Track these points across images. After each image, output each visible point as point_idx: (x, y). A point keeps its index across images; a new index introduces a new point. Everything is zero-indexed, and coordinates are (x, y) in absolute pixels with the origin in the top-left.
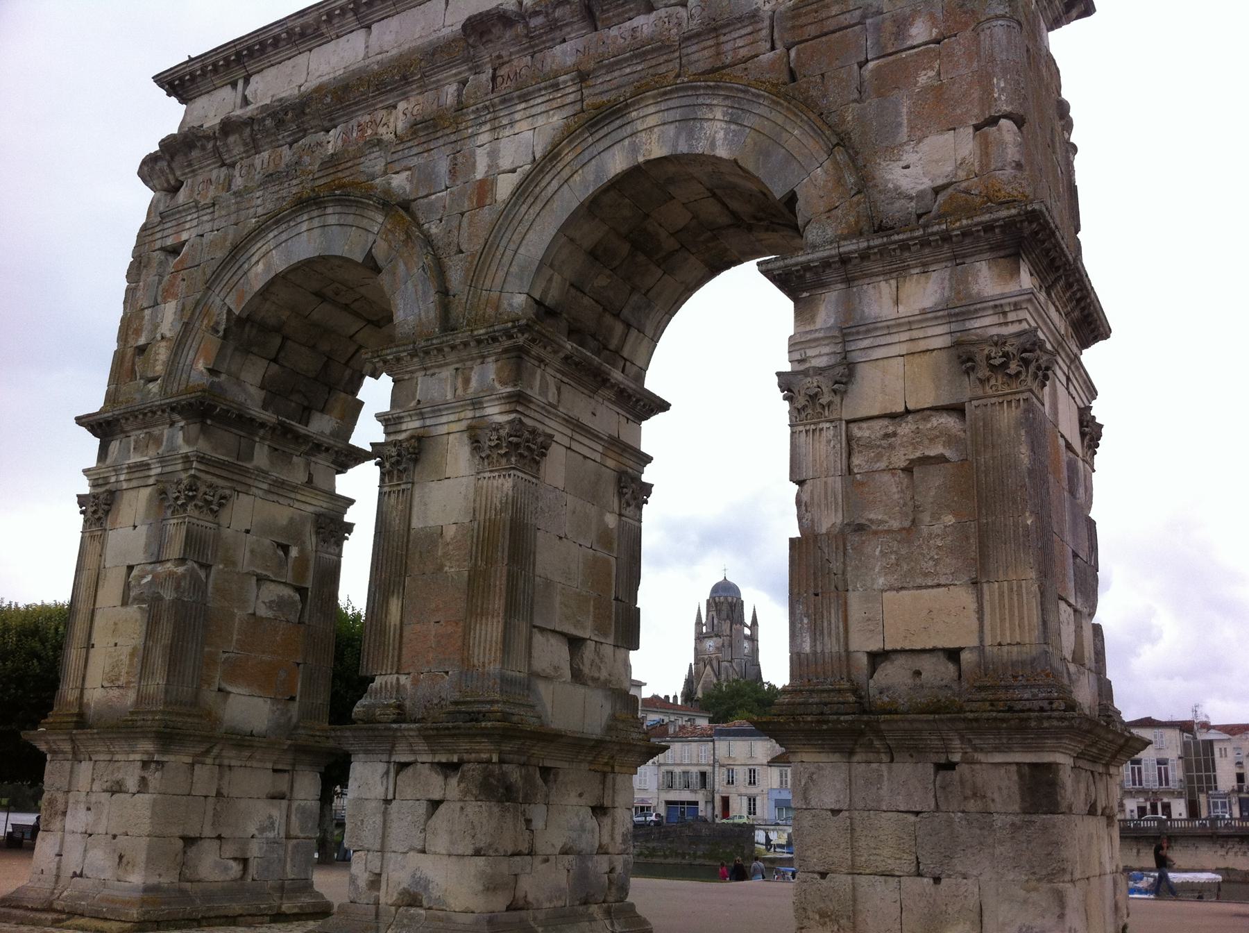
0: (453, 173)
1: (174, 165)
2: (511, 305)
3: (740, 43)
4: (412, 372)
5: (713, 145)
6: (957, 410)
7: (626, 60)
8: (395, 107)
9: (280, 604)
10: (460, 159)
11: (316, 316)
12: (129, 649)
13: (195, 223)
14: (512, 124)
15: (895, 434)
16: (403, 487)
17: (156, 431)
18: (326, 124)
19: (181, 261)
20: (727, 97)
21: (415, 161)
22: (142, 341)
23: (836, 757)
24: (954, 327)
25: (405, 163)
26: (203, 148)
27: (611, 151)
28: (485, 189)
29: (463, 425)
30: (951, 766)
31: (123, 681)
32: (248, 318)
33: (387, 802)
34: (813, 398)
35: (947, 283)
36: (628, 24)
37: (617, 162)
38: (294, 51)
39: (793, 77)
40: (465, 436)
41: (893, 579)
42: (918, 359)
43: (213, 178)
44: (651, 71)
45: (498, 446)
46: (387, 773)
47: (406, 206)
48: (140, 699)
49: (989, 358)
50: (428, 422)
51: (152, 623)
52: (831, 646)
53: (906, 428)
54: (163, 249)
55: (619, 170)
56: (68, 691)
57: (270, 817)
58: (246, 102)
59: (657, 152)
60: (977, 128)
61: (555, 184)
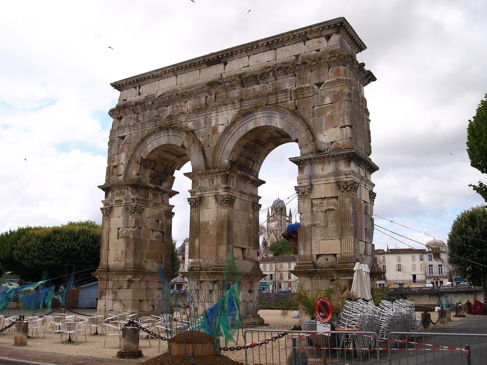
0: (205, 123)
1: (120, 112)
3: (283, 97)
4: (197, 179)
6: (337, 197)
7: (253, 98)
8: (187, 102)
9: (157, 237)
10: (207, 120)
11: (164, 157)
12: (121, 251)
13: (128, 130)
14: (222, 112)
15: (322, 203)
16: (197, 210)
17: (123, 190)
18: (167, 105)
19: (125, 141)
20: (280, 112)
21: (194, 119)
22: (115, 164)
23: (309, 279)
24: (336, 178)
25: (191, 119)
26: (129, 109)
27: (249, 123)
28: (215, 130)
29: (213, 194)
30: (334, 280)
31: (120, 259)
32: (147, 159)
34: (303, 193)
35: (334, 166)
36: (252, 87)
37: (251, 126)
38: (154, 80)
39: (297, 109)
40: (213, 197)
41: (322, 238)
42: (327, 185)
43: (132, 117)
44: (260, 102)
47: (192, 131)
48: (126, 264)
49: (343, 186)
50: (203, 193)
51: (127, 244)
52: (308, 253)
53: (325, 202)
54: (118, 137)
55: (252, 128)
56: (103, 262)
57: (159, 294)
58: (140, 94)
59: (262, 124)
60: (341, 128)
61: (234, 130)
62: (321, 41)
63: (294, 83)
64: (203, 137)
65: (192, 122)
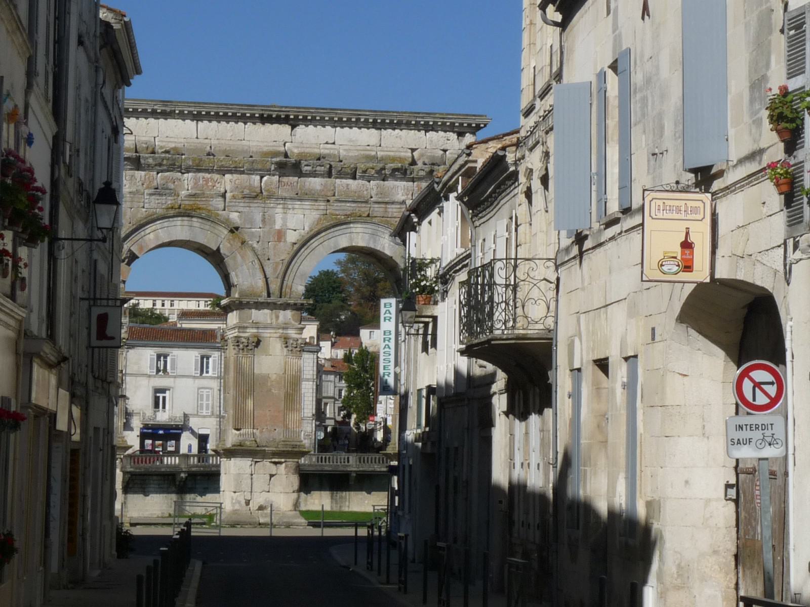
0: (264, 221)
2: (297, 289)
3: (395, 210)
5: (384, 248)
10: (267, 217)
14: (294, 209)
21: (241, 209)
25: (236, 209)
28: (280, 235)
29: (278, 335)
33: (252, 475)
44: (357, 209)
45: (296, 347)
46: (251, 465)
47: (237, 228)
50: (260, 331)
61: (316, 244)
62: (451, 138)
63: (411, 193)
64: (258, 242)
65: (238, 214)
